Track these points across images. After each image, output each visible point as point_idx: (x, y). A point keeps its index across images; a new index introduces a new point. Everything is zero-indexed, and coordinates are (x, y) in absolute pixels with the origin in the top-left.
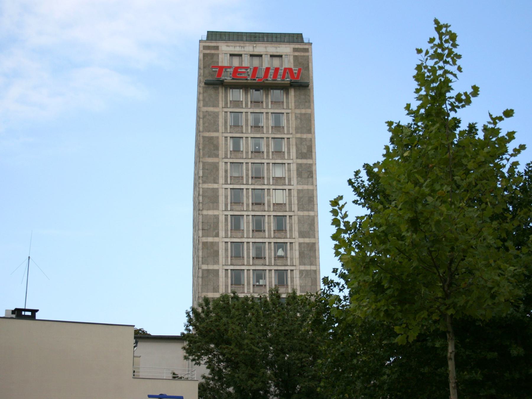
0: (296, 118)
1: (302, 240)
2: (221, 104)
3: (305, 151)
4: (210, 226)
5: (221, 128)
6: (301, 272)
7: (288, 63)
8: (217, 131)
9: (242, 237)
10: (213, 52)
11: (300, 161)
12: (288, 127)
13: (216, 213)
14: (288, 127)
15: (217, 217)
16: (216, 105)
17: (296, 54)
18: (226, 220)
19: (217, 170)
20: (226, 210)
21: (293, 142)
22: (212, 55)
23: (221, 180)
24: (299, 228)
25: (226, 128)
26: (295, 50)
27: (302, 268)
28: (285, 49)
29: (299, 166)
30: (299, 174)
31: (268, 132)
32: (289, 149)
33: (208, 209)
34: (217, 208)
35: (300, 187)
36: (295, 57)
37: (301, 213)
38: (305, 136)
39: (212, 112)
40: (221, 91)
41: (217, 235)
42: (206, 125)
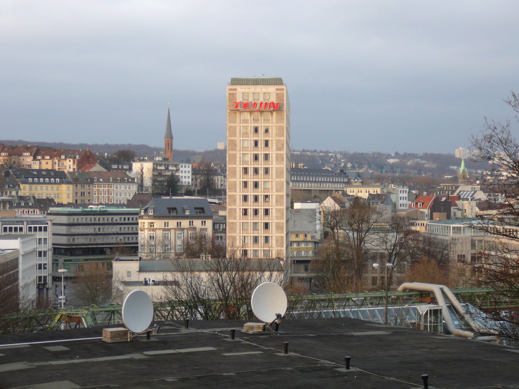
0: (276, 128)
1: (277, 194)
2: (238, 121)
3: (280, 146)
5: (238, 135)
6: (276, 209)
7: (273, 99)
8: (236, 136)
9: (248, 192)
10: (233, 92)
11: (278, 152)
12: (272, 134)
13: (235, 180)
14: (272, 134)
15: (235, 182)
16: (235, 122)
17: (278, 92)
18: (240, 183)
19: (236, 157)
20: (240, 178)
21: (274, 142)
22: (233, 94)
23: (238, 163)
24: (276, 187)
25: (240, 135)
26: (277, 89)
27: (277, 207)
28: (272, 89)
29: (277, 155)
30: (277, 159)
31: (261, 137)
32: (272, 146)
33: (232, 178)
34: (236, 178)
35: (277, 166)
36: (277, 94)
37: (277, 180)
38: (280, 138)
40: (238, 114)
41: (236, 191)
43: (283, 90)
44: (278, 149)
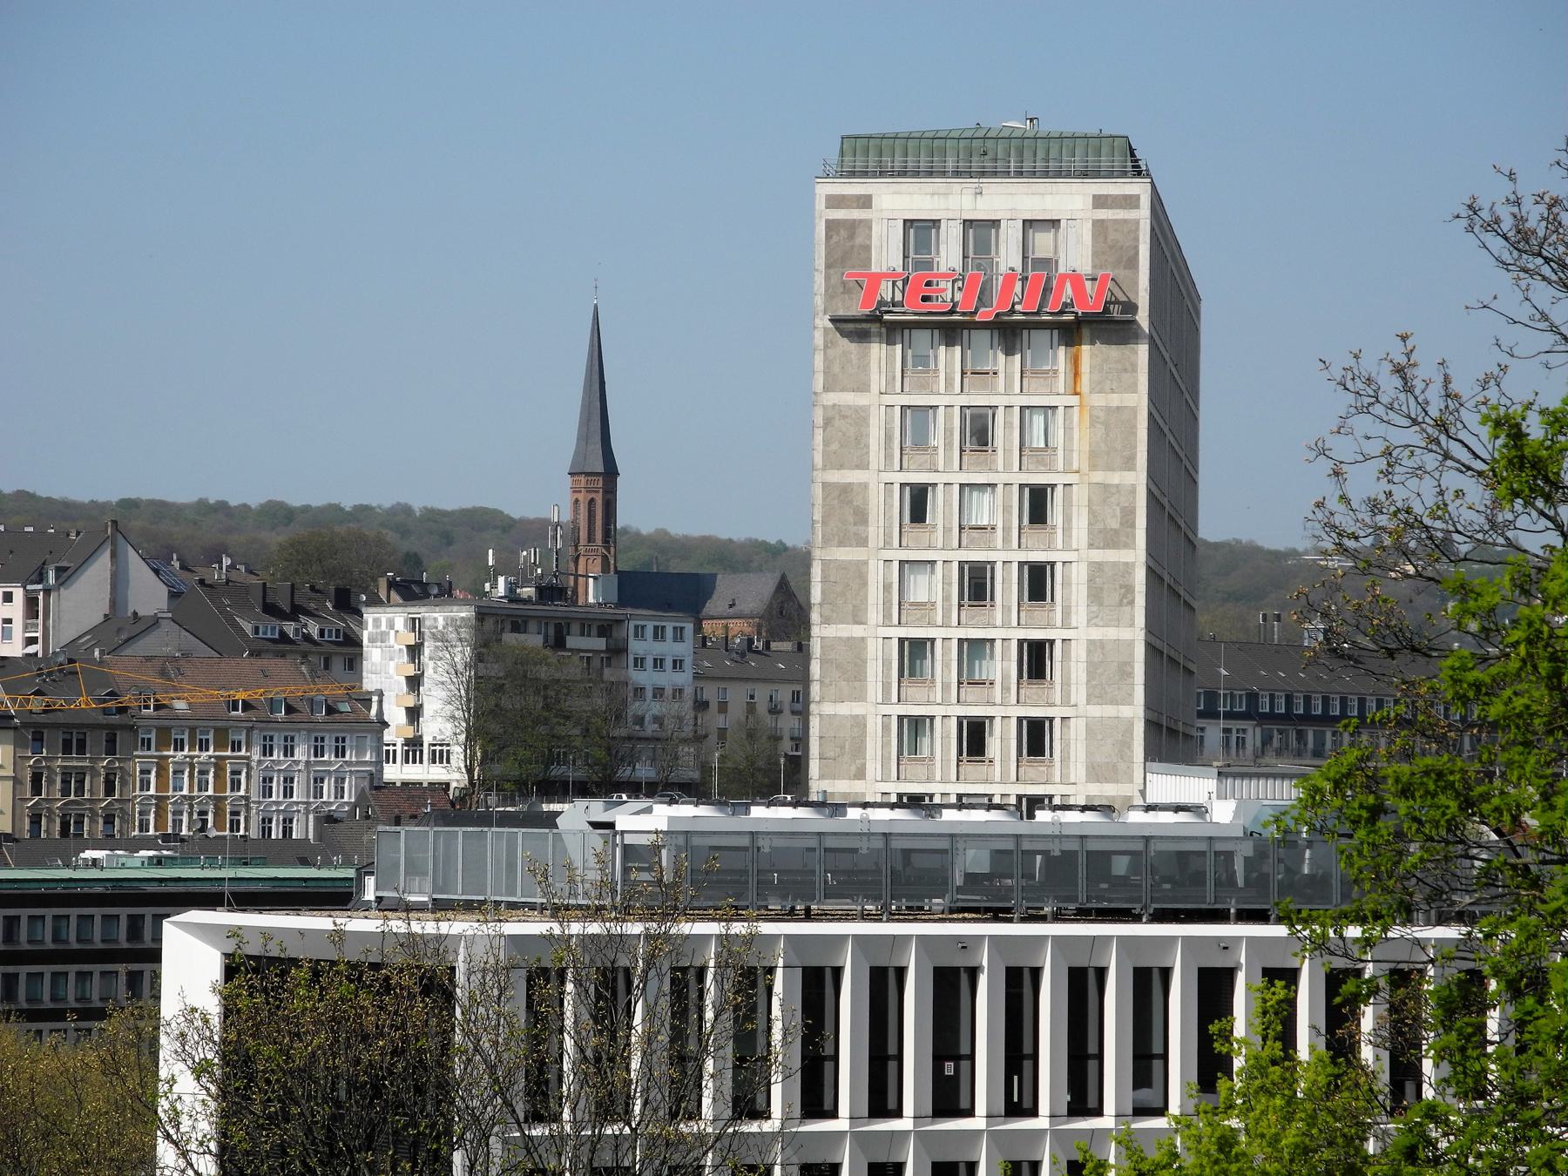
3: (1114, 524)
4: (842, 748)
9: (929, 780)
11: (1098, 555)
12: (1068, 450)
13: (856, 709)
14: (1068, 450)
15: (859, 722)
18: (886, 728)
20: (886, 701)
21: (1080, 495)
22: (852, 227)
24: (1089, 754)
26: (1100, 202)
28: (1070, 200)
29: (1096, 569)
30: (1095, 595)
34: (861, 697)
35: (1096, 634)
36: (1099, 227)
37: (1096, 711)
38: (1115, 478)
39: (849, 407)
42: (834, 447)
43: (1131, 202)
44: (1105, 537)
